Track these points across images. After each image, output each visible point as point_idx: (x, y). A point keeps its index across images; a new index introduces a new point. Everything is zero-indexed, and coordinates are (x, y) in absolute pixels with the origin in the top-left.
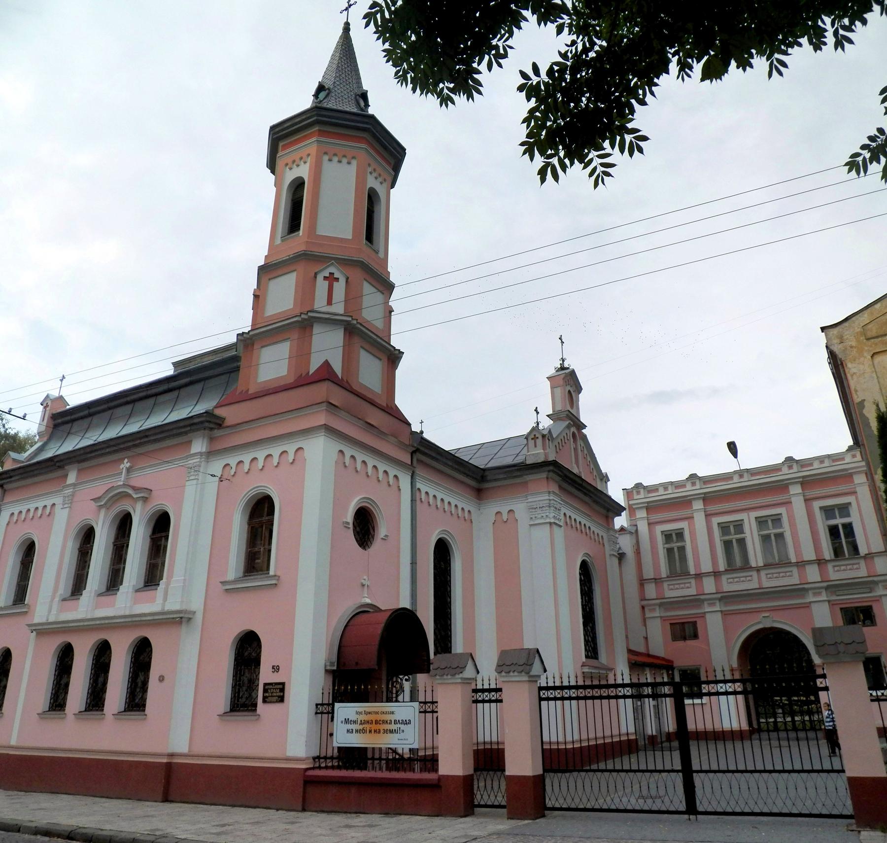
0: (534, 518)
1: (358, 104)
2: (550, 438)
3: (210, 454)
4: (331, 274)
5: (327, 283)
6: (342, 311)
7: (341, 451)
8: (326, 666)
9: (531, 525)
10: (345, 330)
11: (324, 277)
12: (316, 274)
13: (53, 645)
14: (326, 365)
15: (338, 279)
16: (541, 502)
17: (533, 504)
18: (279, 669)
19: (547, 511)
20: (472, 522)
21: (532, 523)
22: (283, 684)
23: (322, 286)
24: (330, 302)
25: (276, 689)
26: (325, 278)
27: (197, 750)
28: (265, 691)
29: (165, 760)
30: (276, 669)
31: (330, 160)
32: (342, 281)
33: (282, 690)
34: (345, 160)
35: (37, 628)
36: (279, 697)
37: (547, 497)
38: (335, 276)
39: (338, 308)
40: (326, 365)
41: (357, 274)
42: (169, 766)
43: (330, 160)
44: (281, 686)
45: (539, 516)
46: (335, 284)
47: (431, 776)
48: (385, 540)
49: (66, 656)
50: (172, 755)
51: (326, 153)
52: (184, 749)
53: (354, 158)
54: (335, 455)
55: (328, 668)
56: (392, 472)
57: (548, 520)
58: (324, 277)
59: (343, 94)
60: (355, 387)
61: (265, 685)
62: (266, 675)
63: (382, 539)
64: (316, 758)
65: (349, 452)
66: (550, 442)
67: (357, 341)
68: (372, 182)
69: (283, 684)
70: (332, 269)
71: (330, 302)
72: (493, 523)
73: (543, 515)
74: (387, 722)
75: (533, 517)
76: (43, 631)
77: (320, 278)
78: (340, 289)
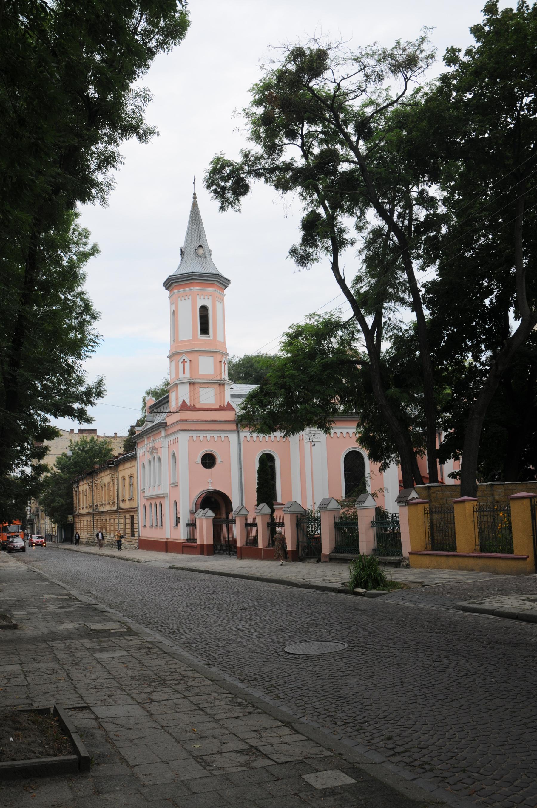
3: (166, 436)
6: (189, 376)
14: (184, 401)
23: (181, 366)
24: (184, 373)
27: (173, 537)
29: (165, 540)
32: (188, 362)
39: (188, 375)
40: (184, 401)
41: (192, 356)
42: (166, 542)
46: (186, 364)
50: (168, 539)
52: (169, 537)
56: (223, 435)
64: (187, 539)
65: (195, 435)
67: (197, 386)
68: (200, 303)
70: (184, 358)
71: (184, 373)
77: (180, 362)
78: (187, 365)
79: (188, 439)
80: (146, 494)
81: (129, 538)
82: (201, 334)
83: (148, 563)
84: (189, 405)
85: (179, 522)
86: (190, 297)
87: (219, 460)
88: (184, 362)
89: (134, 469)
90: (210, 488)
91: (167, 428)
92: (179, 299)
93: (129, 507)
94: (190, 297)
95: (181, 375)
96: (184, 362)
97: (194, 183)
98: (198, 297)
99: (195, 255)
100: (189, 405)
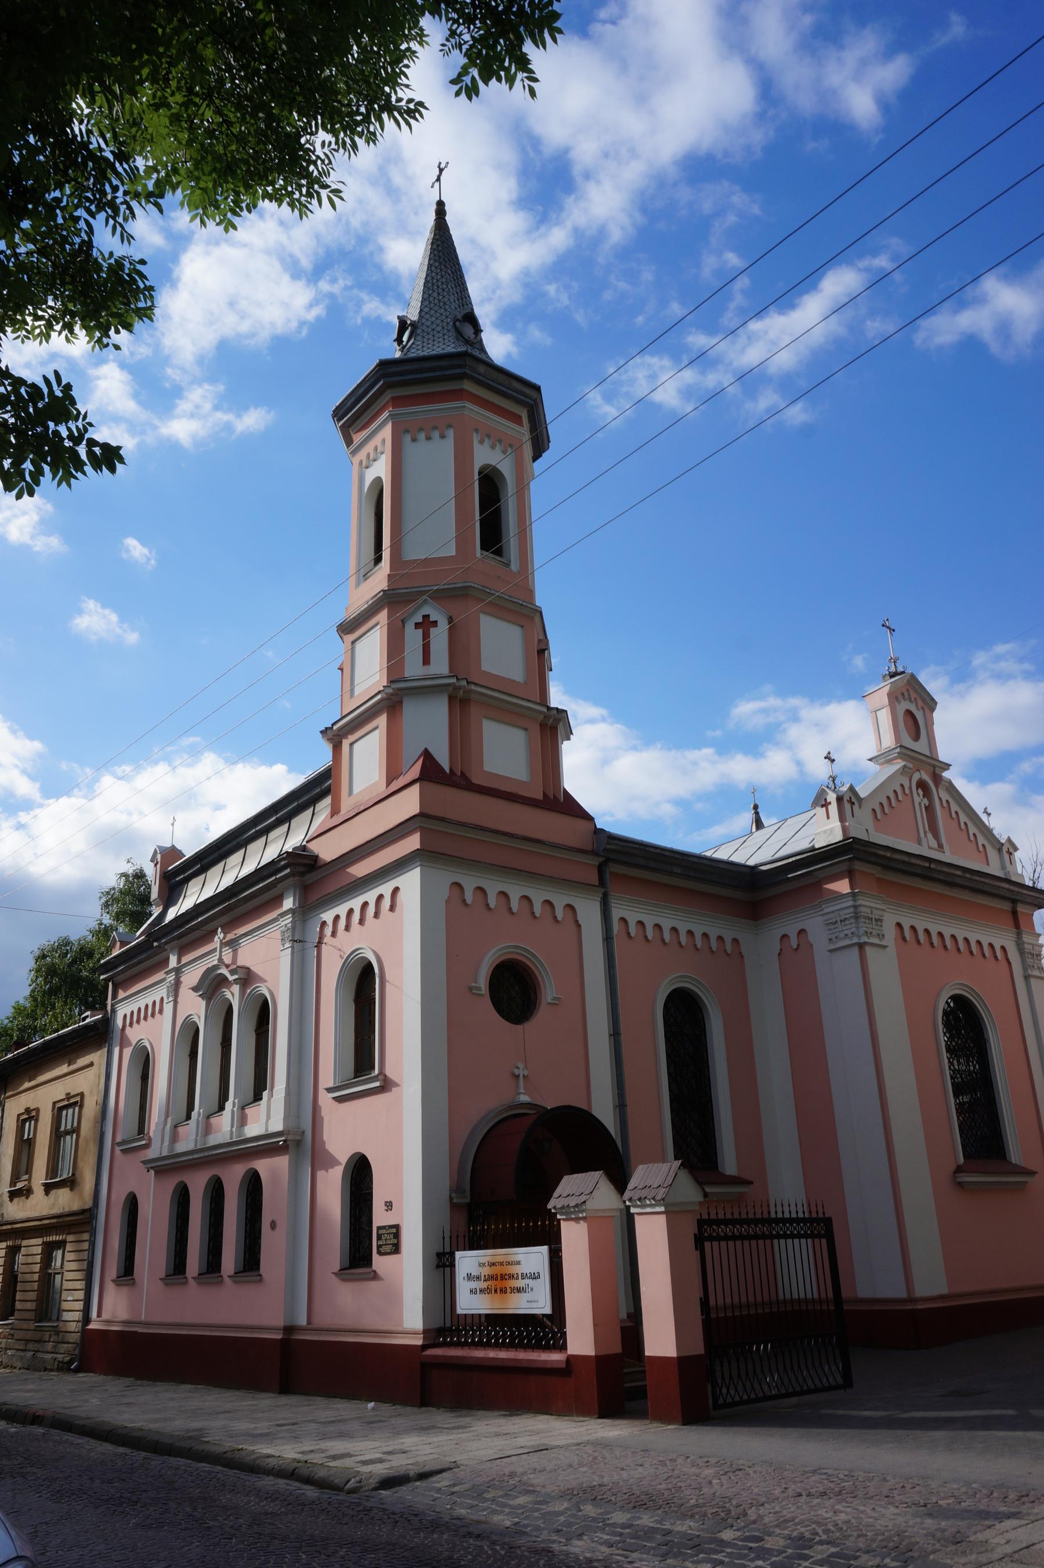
0: (834, 940)
1: (459, 334)
2: (854, 800)
4: (426, 617)
5: (420, 631)
6: (444, 670)
7: (457, 885)
8: (451, 1198)
9: (831, 951)
10: (451, 699)
11: (416, 624)
12: (403, 622)
13: (170, 1184)
15: (436, 622)
16: (841, 912)
17: (831, 916)
18: (392, 1206)
19: (853, 925)
20: (742, 957)
21: (833, 947)
22: (397, 1227)
23: (413, 637)
24: (426, 661)
25: (389, 1234)
26: (417, 625)
28: (379, 1237)
30: (389, 1205)
31: (414, 440)
32: (443, 626)
33: (397, 1235)
34: (436, 434)
35: (153, 1165)
36: (393, 1245)
37: (851, 903)
38: (432, 619)
39: (440, 665)
40: (427, 755)
43: (414, 440)
44: (394, 1230)
45: (842, 935)
46: (432, 630)
47: (555, 1357)
48: (556, 1004)
49: (182, 1198)
51: (407, 431)
53: (449, 426)
54: (444, 892)
55: (455, 1201)
56: (560, 901)
57: (855, 940)
58: (416, 624)
59: (434, 326)
60: (476, 780)
61: (379, 1228)
62: (380, 1218)
63: (549, 1004)
65: (470, 883)
66: (856, 807)
68: (484, 455)
69: (397, 1227)
70: (426, 610)
71: (426, 661)
72: (779, 954)
73: (846, 932)
74: (513, 1276)
75: (833, 936)
76: (162, 1168)
77: (410, 627)
78: (440, 636)
79: (445, 892)
80: (152, 1153)
81: (32, 1325)
82: (481, 549)
83: (404, 1492)
84: (448, 771)
85: (396, 1249)
86: (450, 433)
87: (549, 992)
88: (426, 625)
89: (90, 1074)
90: (524, 1098)
91: (311, 878)
92: (407, 438)
93: (45, 1212)
94: (450, 433)
95: (413, 668)
96: (426, 625)
97: (438, 179)
98: (476, 439)
99: (453, 333)
100: (448, 771)
